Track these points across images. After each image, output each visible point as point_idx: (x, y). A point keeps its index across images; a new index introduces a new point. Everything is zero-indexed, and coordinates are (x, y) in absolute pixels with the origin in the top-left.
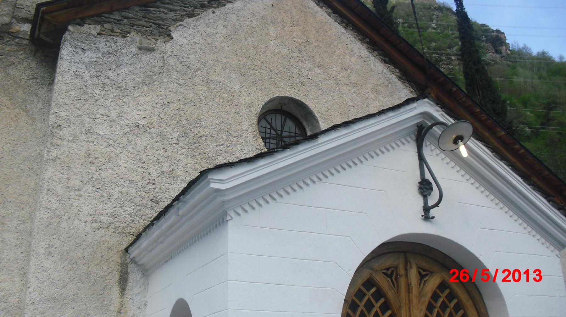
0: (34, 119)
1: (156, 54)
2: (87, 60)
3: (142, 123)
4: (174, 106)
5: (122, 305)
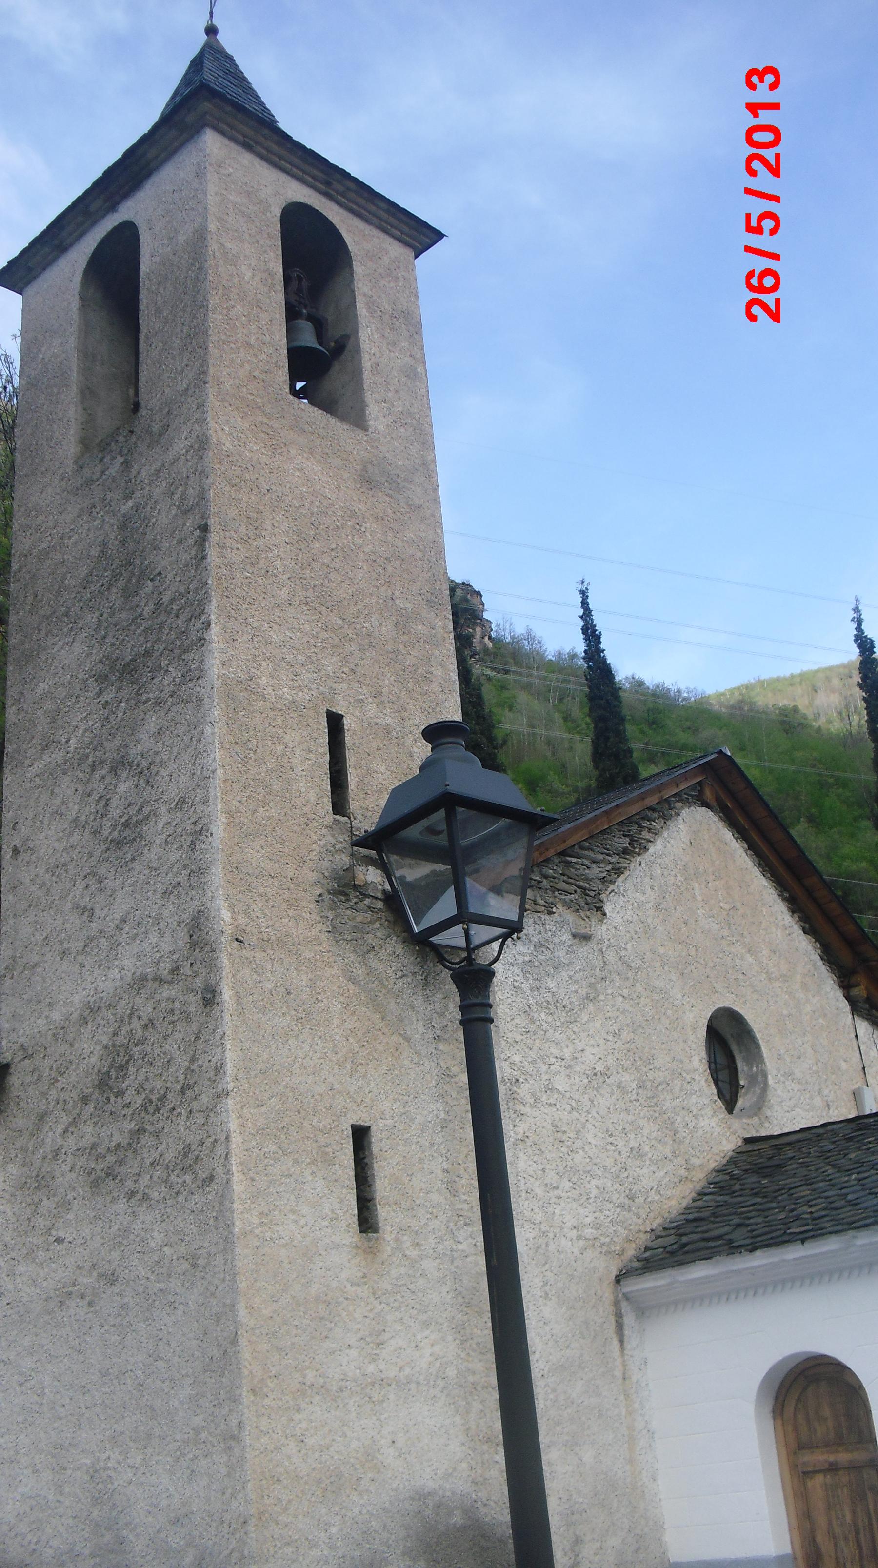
0: (418, 1054)
1: (593, 944)
2: (520, 959)
3: (599, 1067)
4: (625, 1035)
5: (624, 1365)
